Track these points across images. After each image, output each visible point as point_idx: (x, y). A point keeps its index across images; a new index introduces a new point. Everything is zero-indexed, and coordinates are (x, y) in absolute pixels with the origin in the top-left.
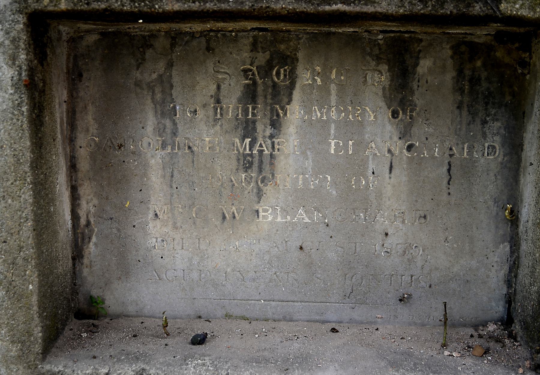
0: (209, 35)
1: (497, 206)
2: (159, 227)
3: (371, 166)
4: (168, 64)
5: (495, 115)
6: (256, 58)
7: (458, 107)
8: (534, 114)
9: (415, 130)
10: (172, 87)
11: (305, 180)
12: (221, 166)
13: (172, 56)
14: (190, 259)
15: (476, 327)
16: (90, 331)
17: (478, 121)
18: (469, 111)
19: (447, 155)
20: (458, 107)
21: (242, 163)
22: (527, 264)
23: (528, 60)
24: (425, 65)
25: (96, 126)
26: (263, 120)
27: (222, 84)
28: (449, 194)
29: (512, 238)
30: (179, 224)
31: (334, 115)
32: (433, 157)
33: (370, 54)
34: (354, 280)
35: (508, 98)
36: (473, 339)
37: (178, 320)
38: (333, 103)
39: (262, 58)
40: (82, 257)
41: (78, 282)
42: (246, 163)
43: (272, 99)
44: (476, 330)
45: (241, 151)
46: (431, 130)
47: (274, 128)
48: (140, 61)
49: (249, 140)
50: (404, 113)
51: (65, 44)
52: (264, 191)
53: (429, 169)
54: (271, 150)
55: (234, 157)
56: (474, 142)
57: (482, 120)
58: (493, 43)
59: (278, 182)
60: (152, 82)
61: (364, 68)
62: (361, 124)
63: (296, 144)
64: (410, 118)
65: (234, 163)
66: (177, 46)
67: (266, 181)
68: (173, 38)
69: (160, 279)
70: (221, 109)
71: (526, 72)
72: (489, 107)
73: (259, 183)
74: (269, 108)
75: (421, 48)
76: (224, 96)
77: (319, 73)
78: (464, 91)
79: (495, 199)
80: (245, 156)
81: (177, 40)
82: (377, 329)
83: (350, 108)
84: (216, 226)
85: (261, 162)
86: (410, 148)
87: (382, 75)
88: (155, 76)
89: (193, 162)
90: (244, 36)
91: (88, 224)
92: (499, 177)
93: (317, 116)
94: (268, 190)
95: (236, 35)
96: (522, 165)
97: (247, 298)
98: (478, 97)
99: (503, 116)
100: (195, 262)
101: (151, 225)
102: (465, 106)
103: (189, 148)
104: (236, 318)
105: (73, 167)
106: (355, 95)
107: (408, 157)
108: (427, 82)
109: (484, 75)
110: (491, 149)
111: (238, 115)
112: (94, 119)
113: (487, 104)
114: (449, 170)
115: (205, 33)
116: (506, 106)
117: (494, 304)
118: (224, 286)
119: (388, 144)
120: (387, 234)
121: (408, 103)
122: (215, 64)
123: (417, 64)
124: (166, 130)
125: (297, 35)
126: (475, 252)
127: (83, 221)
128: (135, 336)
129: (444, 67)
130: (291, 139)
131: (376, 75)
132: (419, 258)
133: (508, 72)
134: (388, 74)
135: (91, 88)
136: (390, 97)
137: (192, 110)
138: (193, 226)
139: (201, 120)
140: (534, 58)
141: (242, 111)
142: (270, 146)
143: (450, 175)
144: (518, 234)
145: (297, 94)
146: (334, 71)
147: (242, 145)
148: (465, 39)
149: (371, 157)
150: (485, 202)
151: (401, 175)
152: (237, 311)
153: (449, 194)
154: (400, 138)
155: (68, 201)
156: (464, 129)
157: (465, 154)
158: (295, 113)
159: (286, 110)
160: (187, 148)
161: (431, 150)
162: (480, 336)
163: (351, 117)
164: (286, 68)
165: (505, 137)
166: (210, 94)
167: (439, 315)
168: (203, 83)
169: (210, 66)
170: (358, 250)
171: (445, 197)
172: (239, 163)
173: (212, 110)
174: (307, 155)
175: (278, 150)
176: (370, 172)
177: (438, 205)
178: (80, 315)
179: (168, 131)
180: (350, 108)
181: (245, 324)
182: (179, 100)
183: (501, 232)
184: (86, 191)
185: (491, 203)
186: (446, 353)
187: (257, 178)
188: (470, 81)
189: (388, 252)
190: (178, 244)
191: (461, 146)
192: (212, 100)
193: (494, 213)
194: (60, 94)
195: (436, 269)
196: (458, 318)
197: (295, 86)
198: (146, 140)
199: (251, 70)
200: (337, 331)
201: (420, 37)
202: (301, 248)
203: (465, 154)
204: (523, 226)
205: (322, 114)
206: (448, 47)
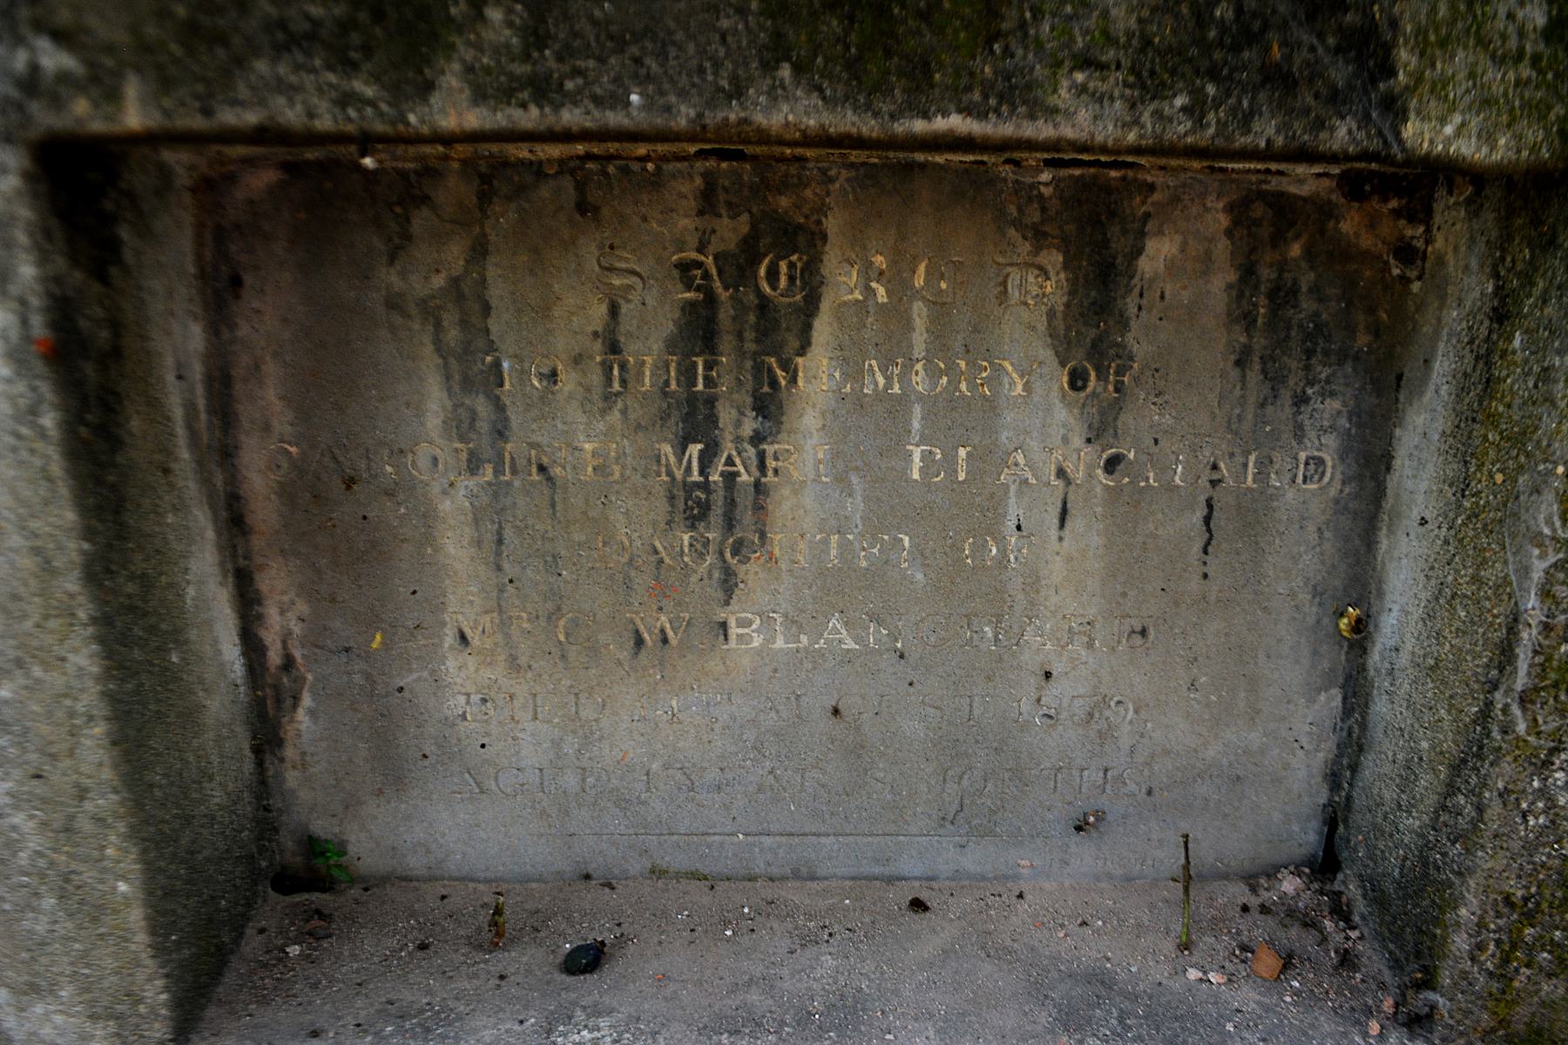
0: (582, 168)
1: (1320, 604)
2: (472, 669)
3: (1014, 510)
4: (473, 249)
5: (1328, 382)
6: (714, 231)
7: (1238, 363)
8: (1432, 387)
9: (1127, 419)
10: (486, 309)
11: (844, 546)
12: (627, 513)
13: (482, 226)
14: (557, 744)
15: (1251, 880)
16: (311, 934)
17: (1286, 397)
18: (1264, 371)
19: (1203, 483)
20: (1238, 363)
21: (681, 506)
22: (1390, 754)
23: (1420, 244)
24: (1158, 253)
25: (290, 415)
26: (735, 396)
27: (621, 301)
28: (1205, 576)
29: (1348, 678)
30: (523, 661)
31: (919, 380)
32: (1171, 488)
33: (1018, 224)
34: (965, 782)
35: (1363, 340)
36: (1248, 917)
37: (534, 885)
38: (919, 350)
39: (730, 231)
40: (280, 743)
41: (276, 802)
42: (692, 506)
43: (757, 341)
44: (1254, 890)
45: (679, 474)
46: (1168, 420)
47: (765, 417)
48: (397, 241)
49: (700, 446)
50: (1102, 375)
51: (187, 198)
52: (741, 576)
53: (1160, 516)
54: (758, 474)
55: (660, 491)
56: (1273, 449)
57: (1295, 395)
58: (1334, 197)
59: (777, 552)
60: (433, 297)
61: (1000, 260)
62: (991, 406)
63: (820, 455)
64: (1117, 390)
65: (662, 506)
66: (495, 199)
67: (744, 551)
68: (485, 179)
69: (482, 792)
70: (623, 367)
71: (1413, 274)
72: (1313, 361)
73: (728, 555)
74: (749, 364)
75: (1151, 209)
76: (629, 335)
77: (881, 273)
78: (1255, 321)
79: (1315, 587)
80: (689, 488)
81: (495, 182)
82: (1020, 896)
83: (963, 364)
84: (619, 663)
85: (731, 503)
86: (1112, 465)
87: (1048, 278)
88: (439, 281)
89: (553, 505)
90: (680, 171)
91: (288, 664)
92: (1327, 534)
93: (876, 384)
94: (751, 572)
95: (659, 169)
96: (1388, 504)
97: (702, 829)
98: (1288, 337)
99: (1347, 385)
100: (569, 749)
101: (451, 664)
102: (1257, 359)
103: (542, 469)
104: (678, 876)
105: (234, 520)
106: (976, 330)
107: (1107, 487)
108: (1162, 297)
109: (1307, 279)
110: (1312, 467)
111: (667, 383)
112: (282, 398)
113: (1309, 353)
114: (1207, 520)
115: (572, 164)
116: (1356, 358)
117: (1296, 828)
118: (644, 803)
119: (1058, 455)
120: (1048, 675)
121: (1112, 352)
122: (601, 247)
123: (1138, 251)
124: (478, 424)
125: (824, 172)
126: (1258, 712)
127: (274, 657)
128: (423, 947)
129: (1207, 257)
130: (808, 442)
131: (1031, 279)
132: (1126, 728)
133: (1368, 273)
134: (1062, 276)
135: (266, 317)
136: (1065, 337)
137: (545, 370)
138: (561, 665)
139: (571, 396)
140: (1439, 243)
141: (679, 371)
142: (754, 461)
143: (1209, 530)
144: (1364, 670)
145: (823, 329)
146: (922, 268)
147: (680, 461)
148: (1264, 187)
149: (1013, 488)
150: (1292, 594)
151: (1087, 532)
152: (677, 861)
153: (1205, 576)
154: (1089, 441)
155: (228, 611)
156: (1250, 417)
157: (1250, 478)
158: (818, 376)
159: (796, 371)
160: (534, 470)
161: (1165, 470)
162: (1264, 909)
163: (963, 386)
164: (794, 258)
165: (1349, 435)
166: (590, 329)
167: (1172, 860)
168: (571, 300)
169: (589, 252)
170: (976, 712)
171: (1194, 584)
172: (672, 506)
173: (598, 370)
174: (850, 484)
175: (776, 471)
176: (1012, 524)
177: (1177, 604)
178: (286, 882)
179: (483, 426)
180: (963, 364)
181: (699, 894)
182: (508, 345)
183: (1326, 665)
185: (1304, 597)
186: (1193, 974)
187: (722, 543)
188: (1272, 295)
189: (1050, 717)
190: (524, 707)
191: (1239, 459)
192: (598, 346)
193: (1311, 620)
194: (179, 341)
195: (1166, 752)
196: (1211, 860)
197: (818, 308)
198: (424, 452)
199: (699, 265)
200: (926, 909)
201: (1149, 179)
202: (836, 712)
203: (1250, 478)
204: (1383, 659)
205: (889, 379)
206: (1221, 205)
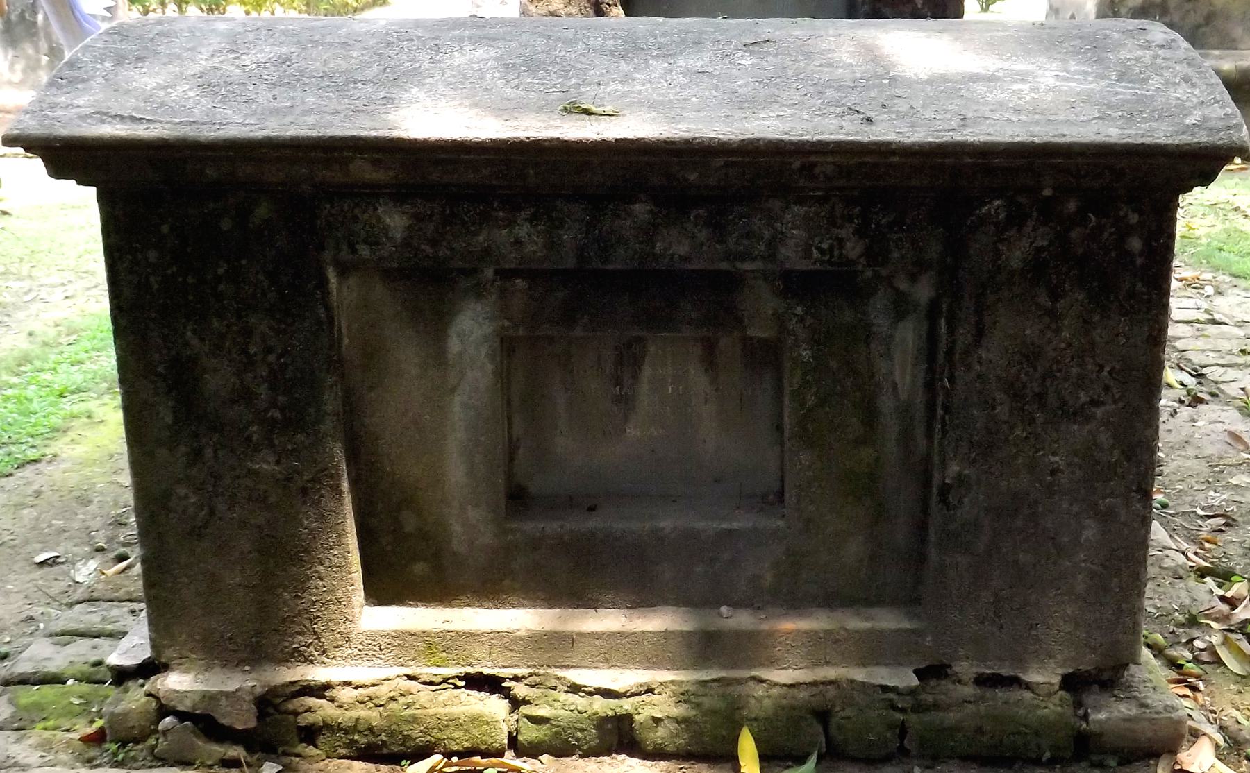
42: (618, 400)
130: (644, 387)
158: (647, 371)
184: (517, 419)
